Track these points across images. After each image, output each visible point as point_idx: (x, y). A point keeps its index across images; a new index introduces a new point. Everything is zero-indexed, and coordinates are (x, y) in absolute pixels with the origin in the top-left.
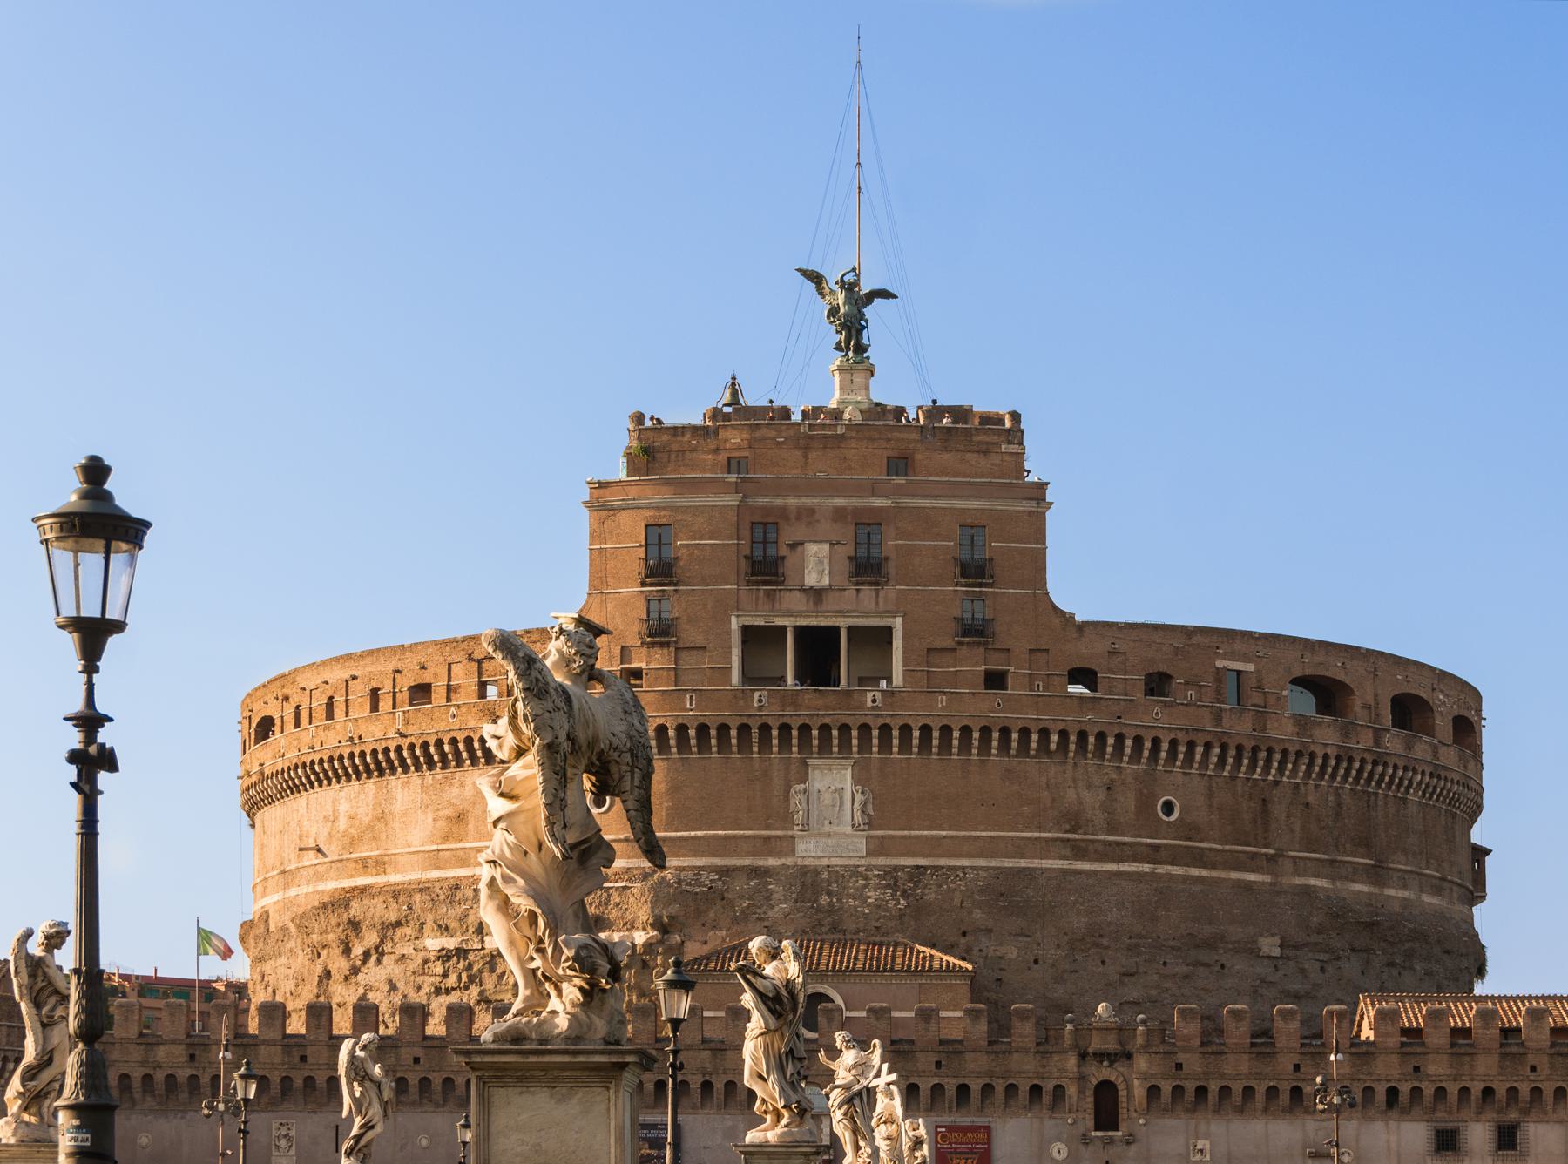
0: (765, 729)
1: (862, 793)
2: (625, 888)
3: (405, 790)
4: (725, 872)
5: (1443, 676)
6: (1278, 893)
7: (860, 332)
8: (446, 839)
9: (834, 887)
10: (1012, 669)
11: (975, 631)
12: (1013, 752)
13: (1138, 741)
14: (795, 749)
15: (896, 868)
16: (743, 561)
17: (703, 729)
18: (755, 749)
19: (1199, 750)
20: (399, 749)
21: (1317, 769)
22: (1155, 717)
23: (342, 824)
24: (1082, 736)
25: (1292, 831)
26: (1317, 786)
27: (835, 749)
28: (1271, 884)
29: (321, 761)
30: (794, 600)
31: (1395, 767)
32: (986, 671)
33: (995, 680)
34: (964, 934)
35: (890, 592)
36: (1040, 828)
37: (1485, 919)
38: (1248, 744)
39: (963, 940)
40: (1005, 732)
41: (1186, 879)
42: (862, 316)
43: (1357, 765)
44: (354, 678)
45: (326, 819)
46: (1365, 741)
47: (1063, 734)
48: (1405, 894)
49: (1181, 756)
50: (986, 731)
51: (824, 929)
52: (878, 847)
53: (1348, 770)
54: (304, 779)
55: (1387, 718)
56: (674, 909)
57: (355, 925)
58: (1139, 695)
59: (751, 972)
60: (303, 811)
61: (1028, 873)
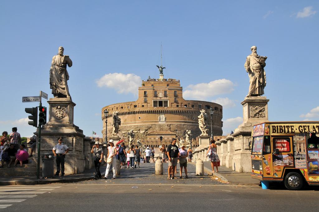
4: (152, 125)
5: (219, 105)
13: (191, 112)
17: (150, 111)
24: (186, 111)
35: (167, 98)
37: (223, 128)
40: (179, 111)
47: (184, 111)
58: (191, 107)
59: (187, 133)
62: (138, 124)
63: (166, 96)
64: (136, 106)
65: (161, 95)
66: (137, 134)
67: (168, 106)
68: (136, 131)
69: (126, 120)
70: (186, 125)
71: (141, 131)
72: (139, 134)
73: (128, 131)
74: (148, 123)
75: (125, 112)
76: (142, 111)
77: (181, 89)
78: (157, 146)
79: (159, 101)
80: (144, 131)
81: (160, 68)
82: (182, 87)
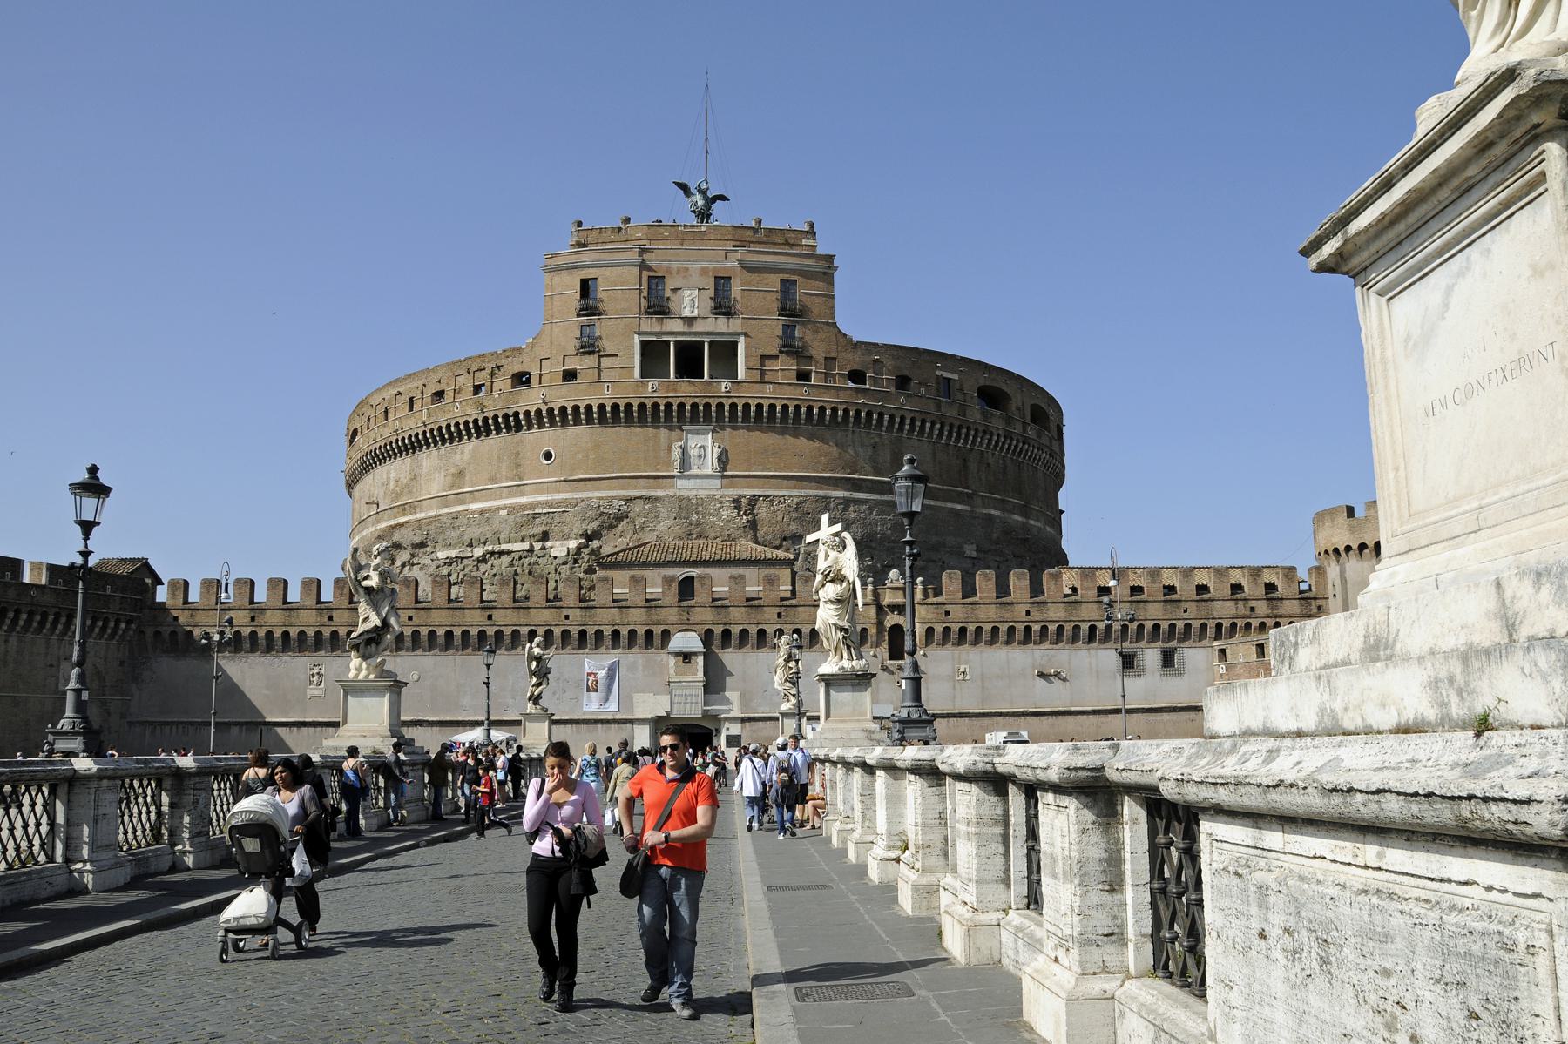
1: (719, 447)
2: (564, 512)
3: (428, 459)
4: (629, 500)
6: (975, 518)
8: (451, 488)
11: (791, 348)
12: (814, 422)
13: (892, 417)
14: (675, 420)
15: (741, 496)
16: (642, 299)
17: (615, 407)
19: (928, 425)
20: (424, 432)
22: (901, 403)
24: (858, 413)
25: (981, 479)
26: (993, 454)
27: (701, 419)
29: (380, 447)
30: (675, 325)
31: (1034, 447)
32: (798, 370)
33: (803, 376)
35: (735, 324)
36: (832, 471)
38: (957, 423)
39: (784, 543)
40: (810, 409)
43: (1015, 442)
44: (400, 393)
45: (383, 484)
46: (1018, 429)
47: (846, 411)
48: (1039, 525)
49: (917, 429)
50: (797, 408)
51: (694, 536)
53: (1010, 445)
55: (1029, 421)
56: (595, 525)
57: (397, 546)
58: (892, 389)
60: (371, 482)
62: (539, 495)
63: (723, 307)
64: (528, 382)
65: (690, 301)
66: (527, 561)
67: (741, 374)
68: (526, 546)
69: (461, 473)
70: (856, 501)
71: (558, 543)
72: (540, 561)
73: (471, 545)
74: (598, 489)
75: (457, 424)
76: (563, 410)
77: (825, 270)
78: (657, 640)
79: (677, 343)
80: (573, 544)
81: (699, 199)
82: (830, 258)
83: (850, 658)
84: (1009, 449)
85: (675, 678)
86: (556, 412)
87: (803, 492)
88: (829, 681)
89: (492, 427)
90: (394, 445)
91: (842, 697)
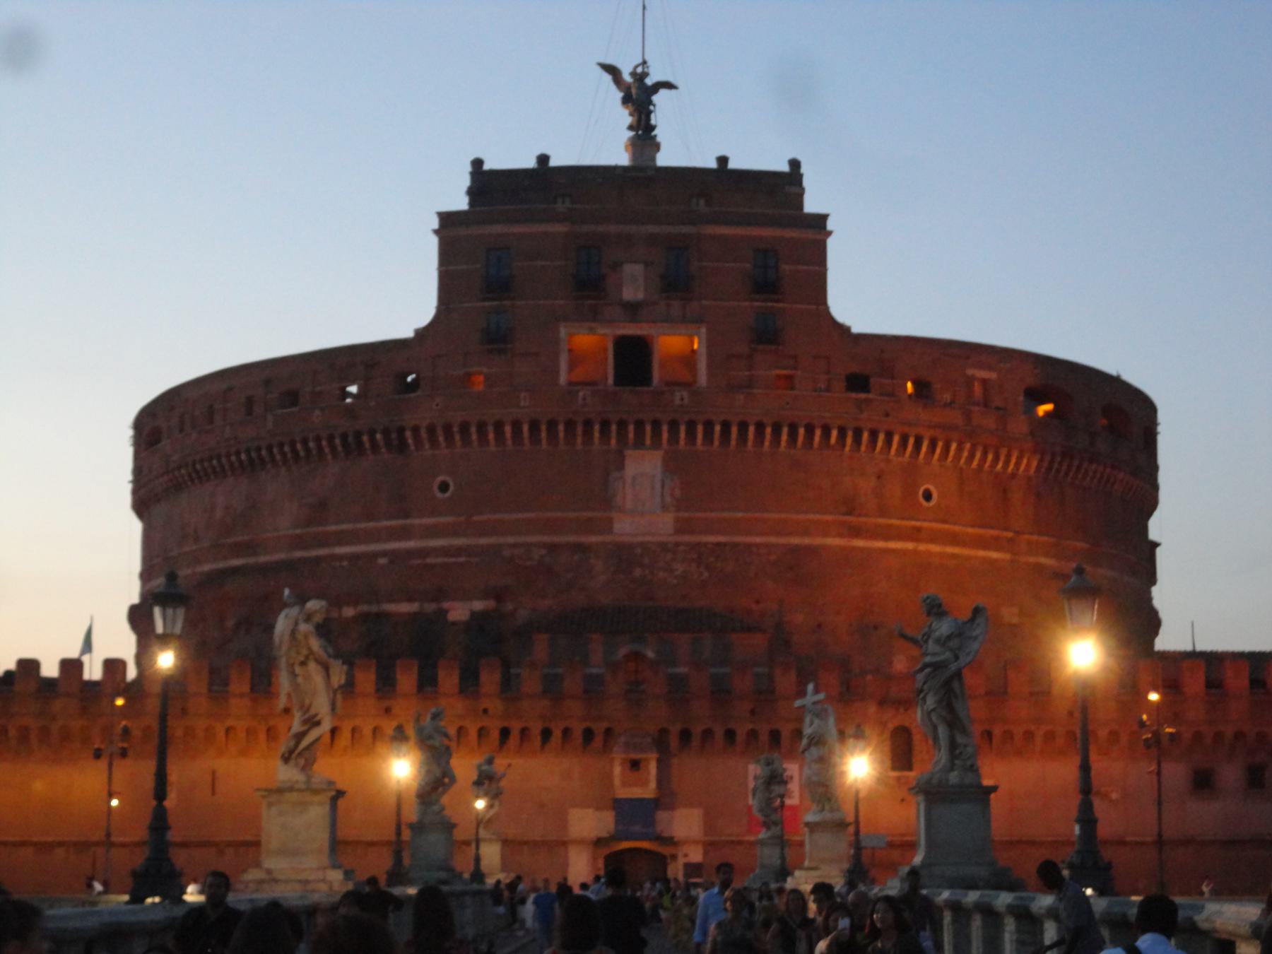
0: (588, 424)
4: (553, 548)
7: (649, 113)
9: (646, 561)
10: (799, 373)
15: (699, 544)
17: (534, 426)
18: (579, 440)
19: (954, 446)
20: (270, 448)
21: (1045, 464)
23: (219, 513)
24: (858, 433)
27: (648, 442)
28: (1012, 561)
29: (202, 461)
34: (758, 602)
41: (942, 556)
42: (650, 103)
43: (1076, 463)
47: (842, 432)
52: (683, 527)
53: (1069, 467)
54: (186, 478)
61: (811, 551)
67: (703, 379)
71: (458, 604)
76: (464, 428)
78: (598, 741)
80: (478, 605)
83: (832, 810)
84: (1067, 474)
85: (623, 793)
86: (455, 429)
87: (782, 540)
88: (813, 827)
89: (367, 445)
90: (224, 460)
91: (824, 839)
